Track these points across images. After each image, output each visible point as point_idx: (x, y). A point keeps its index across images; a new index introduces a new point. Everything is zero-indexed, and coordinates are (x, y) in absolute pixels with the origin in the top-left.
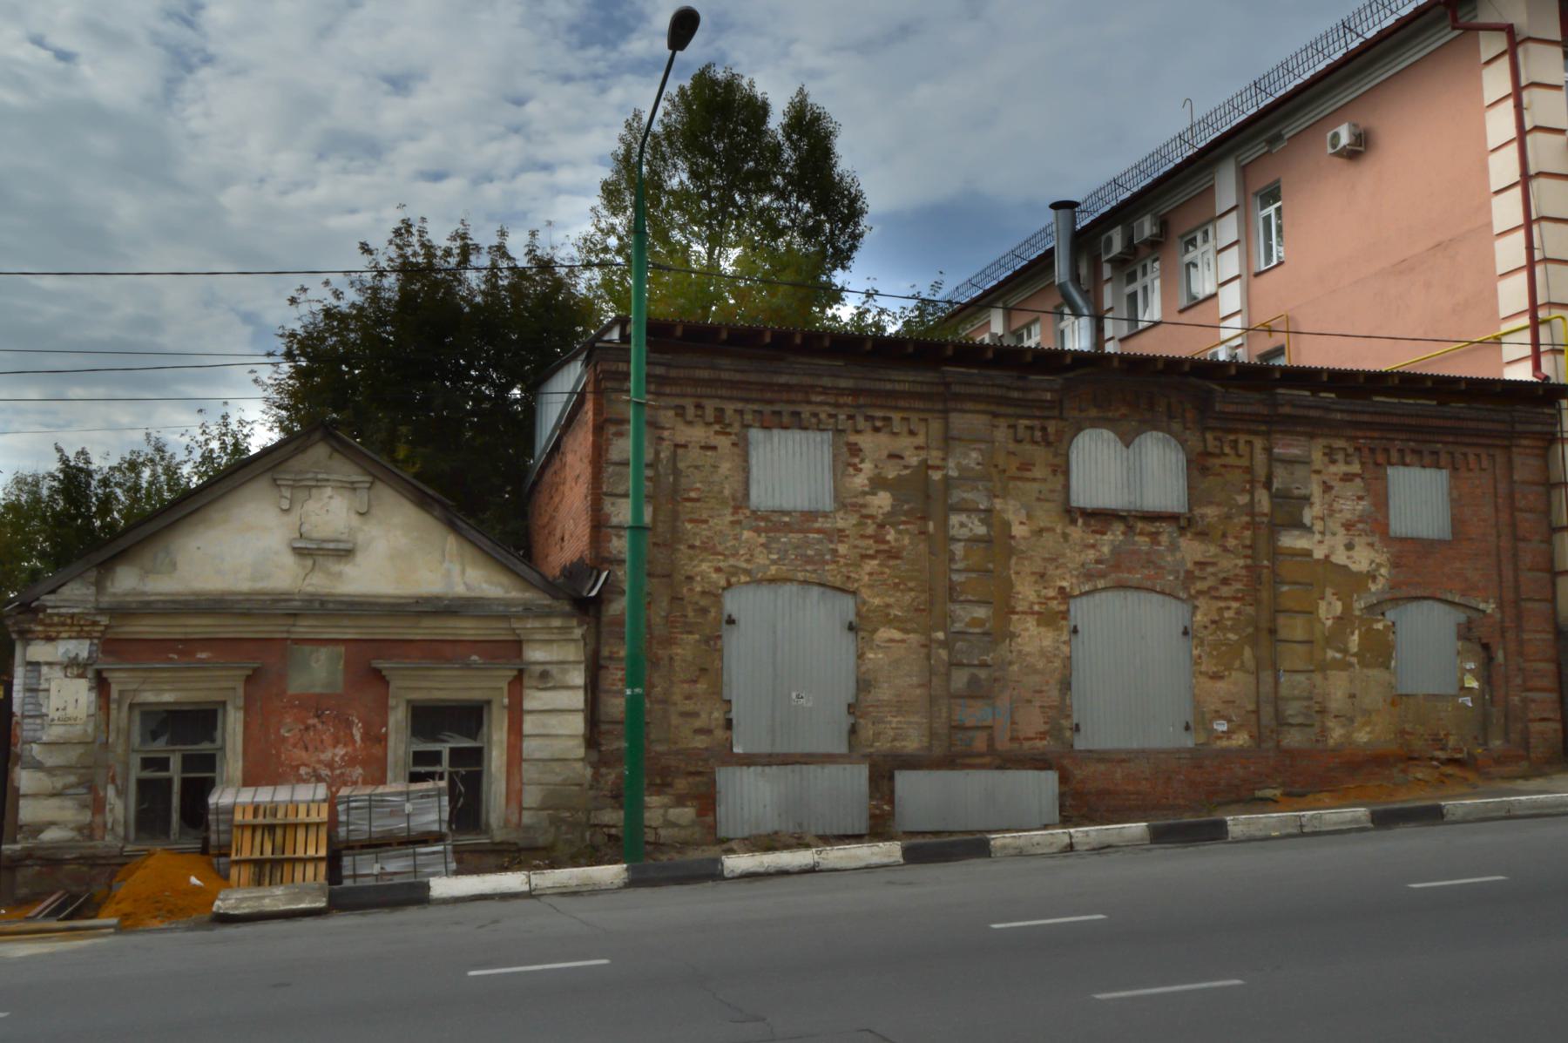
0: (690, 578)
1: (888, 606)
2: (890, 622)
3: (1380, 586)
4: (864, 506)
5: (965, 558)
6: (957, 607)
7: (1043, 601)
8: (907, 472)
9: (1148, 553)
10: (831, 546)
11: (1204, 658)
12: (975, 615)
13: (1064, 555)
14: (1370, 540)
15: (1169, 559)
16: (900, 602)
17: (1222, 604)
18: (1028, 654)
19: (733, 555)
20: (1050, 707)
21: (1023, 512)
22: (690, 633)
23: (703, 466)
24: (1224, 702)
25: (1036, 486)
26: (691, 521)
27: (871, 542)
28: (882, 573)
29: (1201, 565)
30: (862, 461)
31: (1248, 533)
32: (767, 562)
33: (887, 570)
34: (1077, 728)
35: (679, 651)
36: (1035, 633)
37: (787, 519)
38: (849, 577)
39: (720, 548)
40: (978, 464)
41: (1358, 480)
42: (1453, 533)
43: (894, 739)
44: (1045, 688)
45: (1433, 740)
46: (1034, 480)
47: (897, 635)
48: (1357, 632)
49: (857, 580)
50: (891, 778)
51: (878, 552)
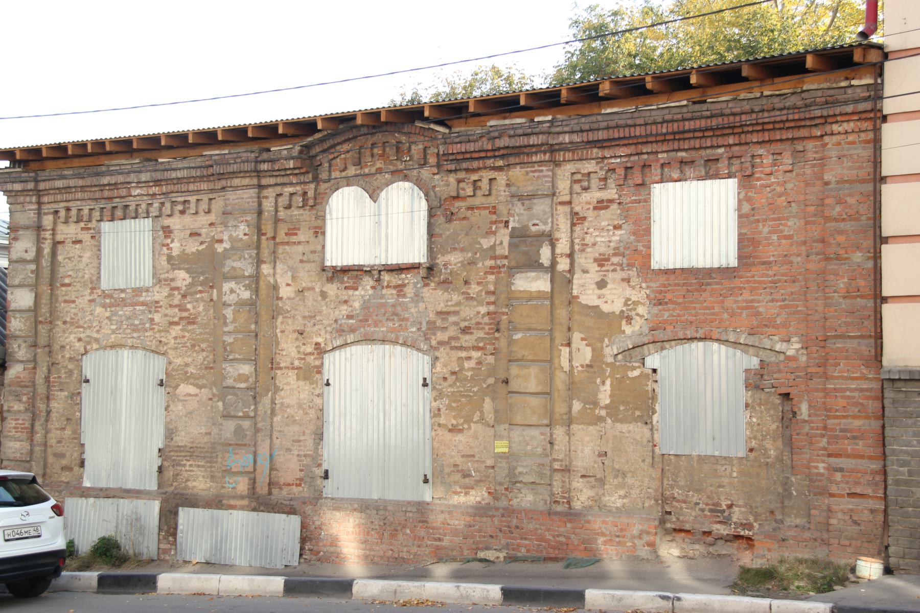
0: (63, 347)
1: (187, 365)
2: (187, 378)
3: (637, 328)
4: (173, 280)
5: (234, 320)
6: (227, 365)
7: (303, 356)
8: (203, 246)
9: (393, 306)
10: (150, 316)
11: (443, 410)
12: (241, 372)
13: (320, 312)
14: (624, 275)
16: (195, 360)
17: (464, 354)
18: (288, 407)
19: (89, 327)
20: (305, 456)
21: (290, 274)
22: (61, 390)
23: (74, 257)
24: (463, 456)
25: (300, 248)
26: (66, 301)
27: (176, 310)
28: (184, 337)
29: (442, 314)
30: (172, 241)
31: (491, 278)
32: (110, 332)
33: (187, 334)
34: (326, 476)
35: (56, 405)
36: (295, 386)
37: (123, 295)
38: (160, 342)
39: (81, 323)
40: (245, 234)
41: (614, 206)
42: (740, 258)
44: (302, 438)
45: (711, 511)
46: (299, 243)
47: (192, 390)
48: (608, 382)
49: (166, 344)
50: (176, 514)
51: (181, 319)
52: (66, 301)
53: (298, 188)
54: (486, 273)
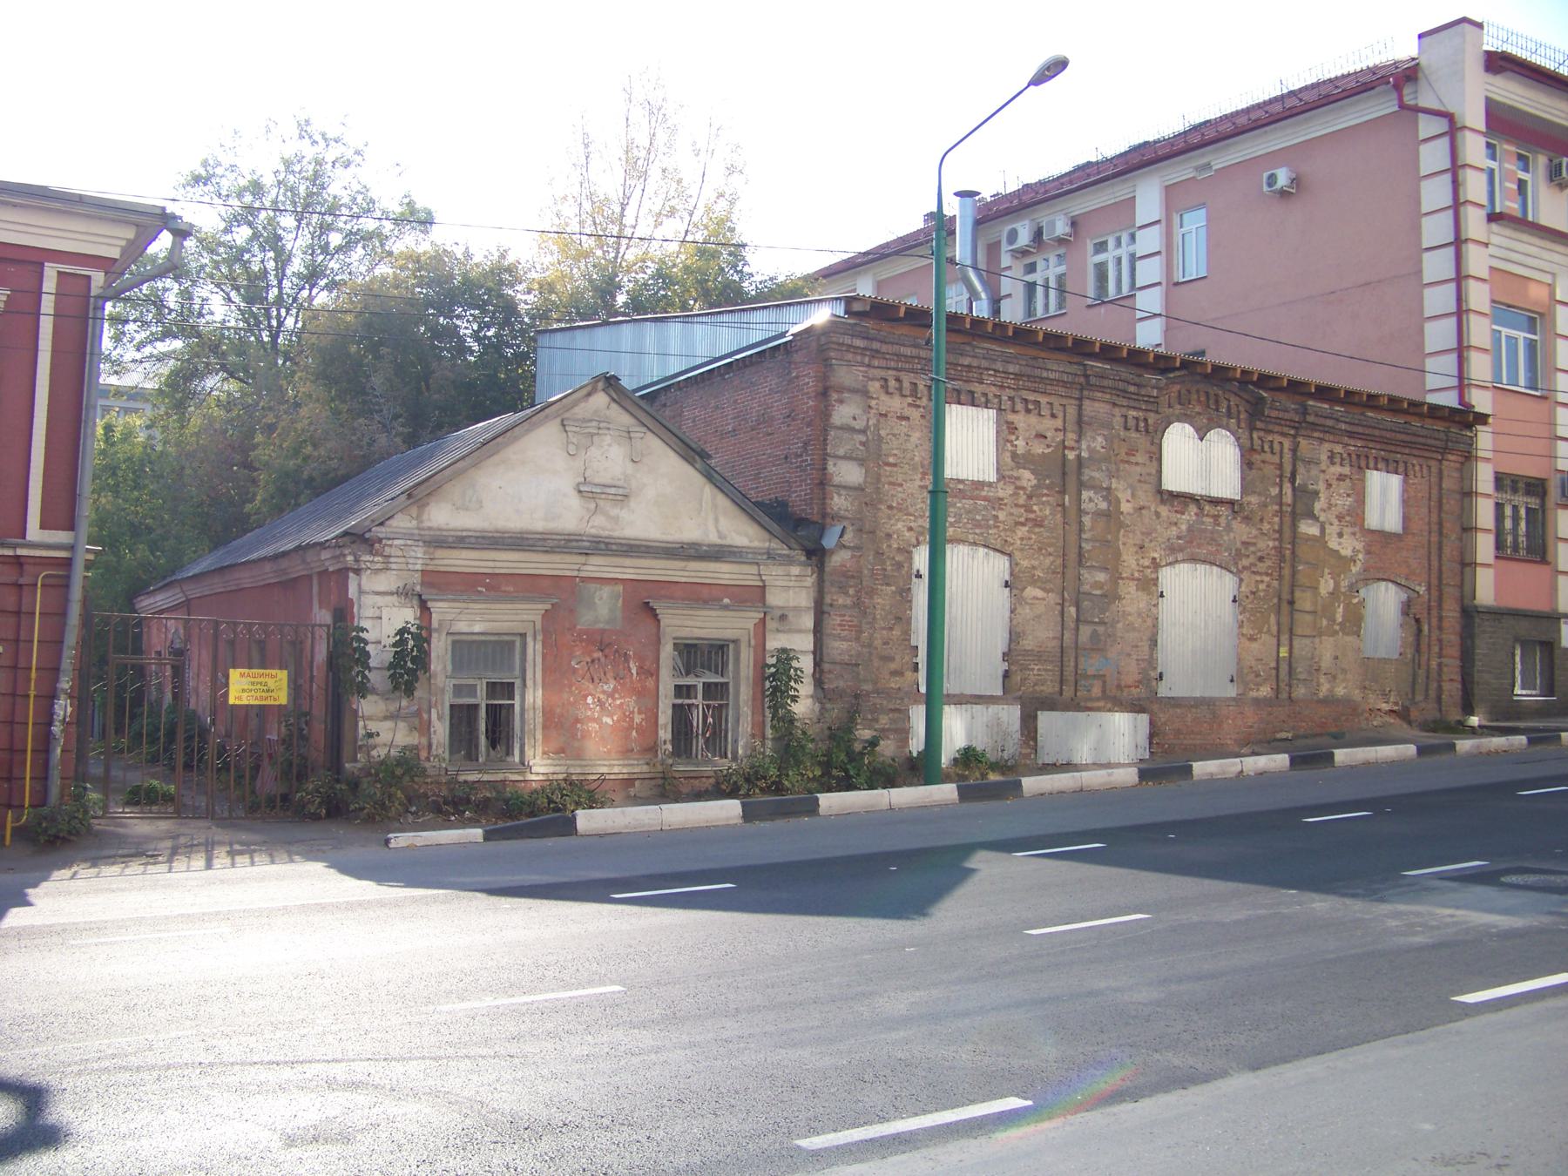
0: (889, 536)
1: (1034, 568)
2: (1034, 582)
4: (1018, 478)
8: (1050, 450)
9: (1212, 533)
10: (994, 513)
12: (1097, 579)
13: (1156, 530)
15: (1226, 538)
17: (1258, 578)
18: (1129, 614)
20: (1143, 660)
21: (1129, 491)
22: (888, 584)
25: (1138, 469)
26: (891, 483)
28: (1030, 539)
30: (1017, 439)
35: (879, 600)
37: (961, 486)
38: (1006, 541)
39: (911, 510)
40: (1103, 447)
43: (1035, 684)
44: (1140, 644)
46: (1137, 464)
47: (1039, 593)
49: (1013, 544)
50: (1035, 717)
52: (891, 483)
53: (1141, 414)
54: (1273, 515)
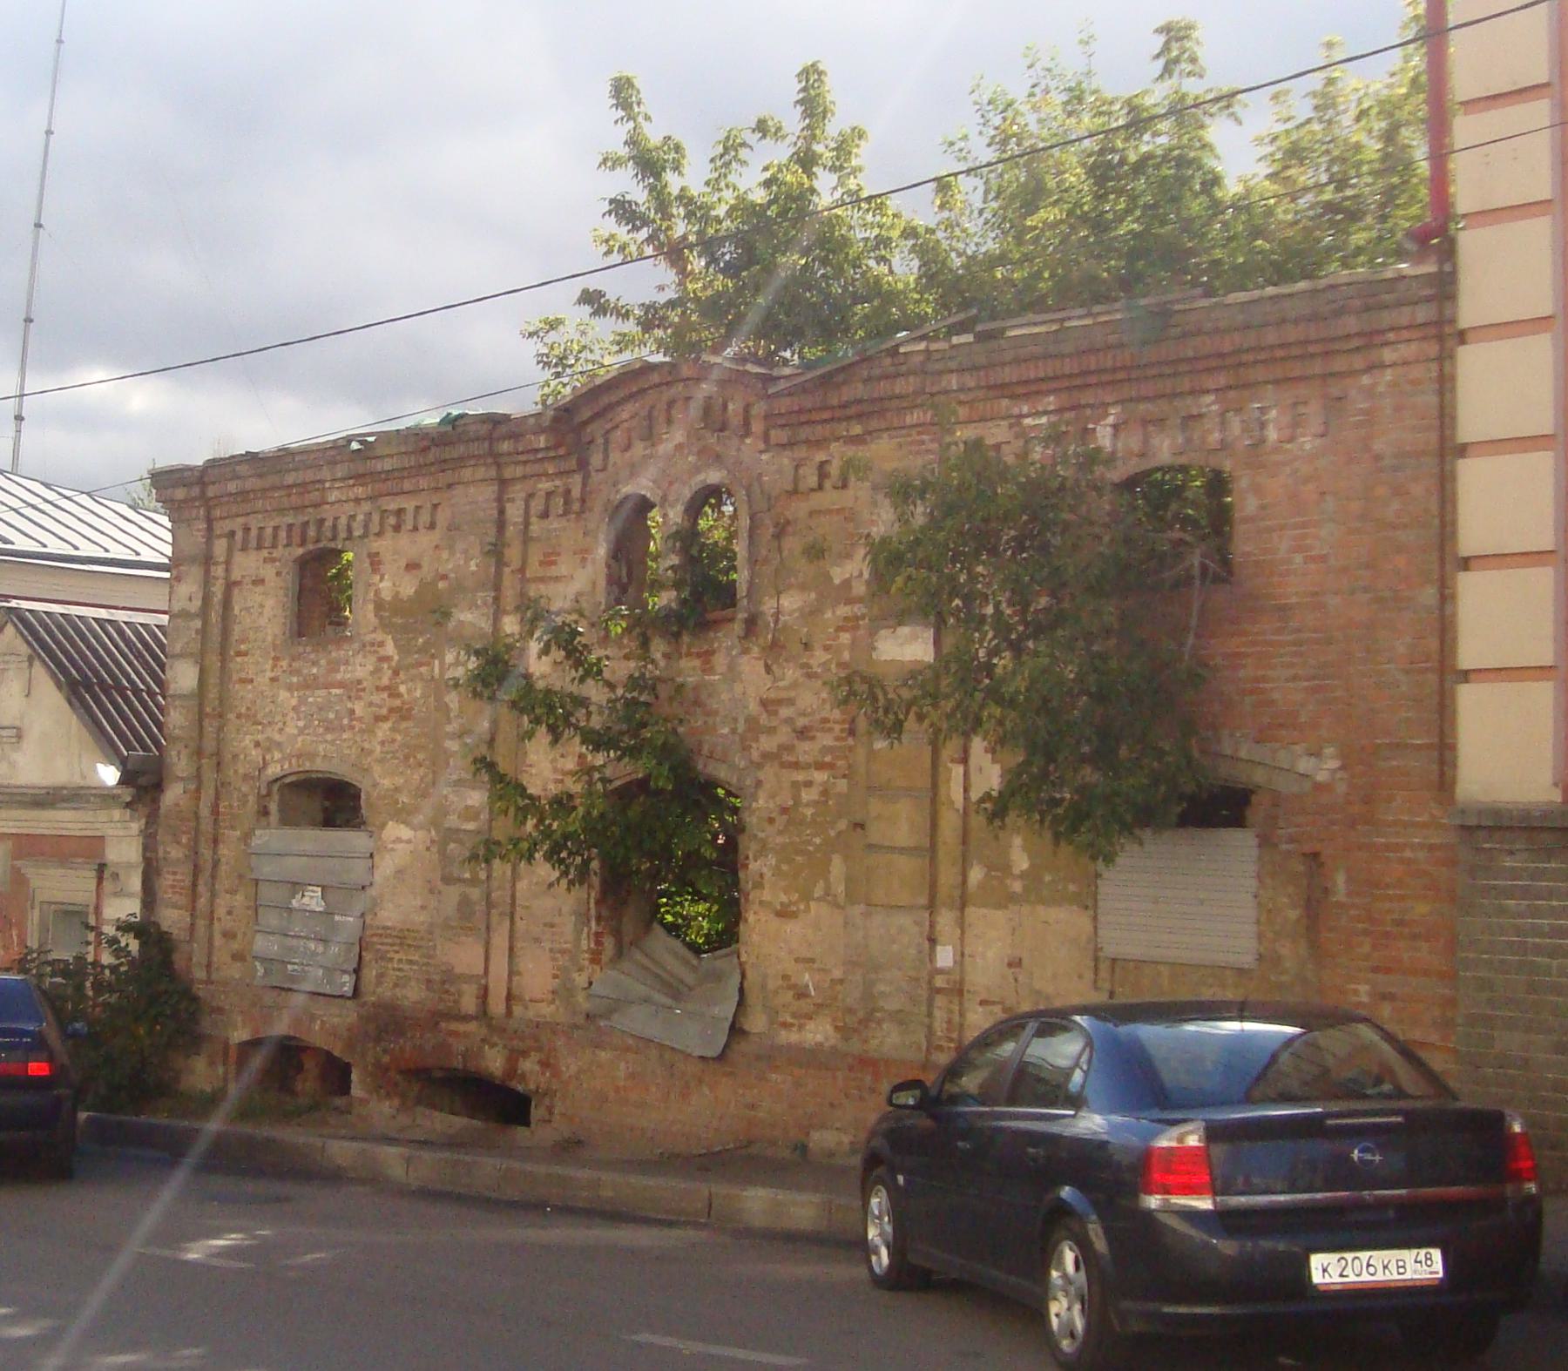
10: (349, 705)
12: (470, 802)
15: (725, 696)
17: (800, 777)
20: (562, 952)
24: (797, 960)
30: (382, 579)
31: (845, 637)
32: (296, 732)
33: (399, 738)
43: (396, 985)
44: (557, 920)
51: (391, 710)
52: (242, 681)
53: (557, 483)
54: (839, 629)
